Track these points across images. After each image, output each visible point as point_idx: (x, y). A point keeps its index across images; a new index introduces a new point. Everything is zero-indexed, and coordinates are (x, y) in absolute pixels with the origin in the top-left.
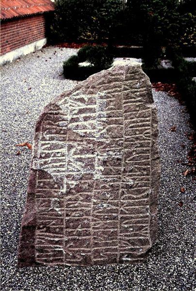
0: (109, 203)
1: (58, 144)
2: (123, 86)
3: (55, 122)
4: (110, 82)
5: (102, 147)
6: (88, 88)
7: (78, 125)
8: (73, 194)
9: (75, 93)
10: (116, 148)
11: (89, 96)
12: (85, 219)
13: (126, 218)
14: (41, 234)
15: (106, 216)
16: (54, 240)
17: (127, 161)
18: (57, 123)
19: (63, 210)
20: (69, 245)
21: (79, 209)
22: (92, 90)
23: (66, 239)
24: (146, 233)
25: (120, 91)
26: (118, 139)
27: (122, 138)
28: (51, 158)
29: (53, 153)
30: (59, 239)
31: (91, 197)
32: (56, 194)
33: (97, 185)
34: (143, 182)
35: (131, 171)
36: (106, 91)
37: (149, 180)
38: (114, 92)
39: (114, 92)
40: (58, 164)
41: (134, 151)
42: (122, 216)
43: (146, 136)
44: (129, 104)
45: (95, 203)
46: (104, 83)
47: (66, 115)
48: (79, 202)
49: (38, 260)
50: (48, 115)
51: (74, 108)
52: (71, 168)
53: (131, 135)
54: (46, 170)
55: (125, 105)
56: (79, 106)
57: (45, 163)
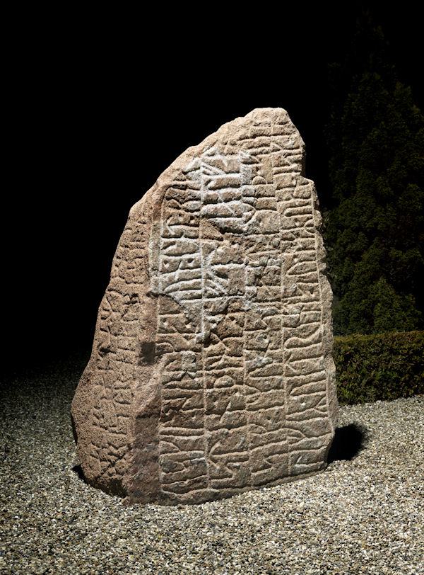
0: (270, 355)
1: (189, 244)
2: (272, 144)
3: (181, 204)
4: (254, 136)
5: (251, 249)
6: (226, 144)
7: (216, 208)
8: (215, 343)
9: (209, 152)
10: (272, 252)
11: (229, 157)
12: (236, 390)
13: (295, 385)
14: (168, 429)
15: (266, 380)
16: (188, 440)
17: (287, 275)
18: (184, 205)
19: (202, 375)
20: (213, 449)
21: (226, 370)
22: (232, 147)
23: (208, 434)
24: (324, 410)
25: (267, 153)
26: (272, 235)
27: (278, 234)
28: (179, 271)
29: (181, 260)
30: (196, 437)
31: (242, 344)
32: (188, 343)
33: (249, 321)
34: (311, 312)
35: (294, 294)
36: (251, 151)
37: (319, 310)
38: (261, 153)
39: (261, 153)
40: (191, 282)
41: (295, 256)
42: (288, 379)
43: (308, 231)
44: (283, 174)
45: (248, 357)
46: (247, 138)
47: (198, 189)
48: (224, 356)
49: (165, 489)
50: (172, 189)
51: (209, 177)
52: (211, 291)
53: (289, 229)
54: (171, 294)
55: (276, 176)
56: (216, 174)
57: (171, 282)
